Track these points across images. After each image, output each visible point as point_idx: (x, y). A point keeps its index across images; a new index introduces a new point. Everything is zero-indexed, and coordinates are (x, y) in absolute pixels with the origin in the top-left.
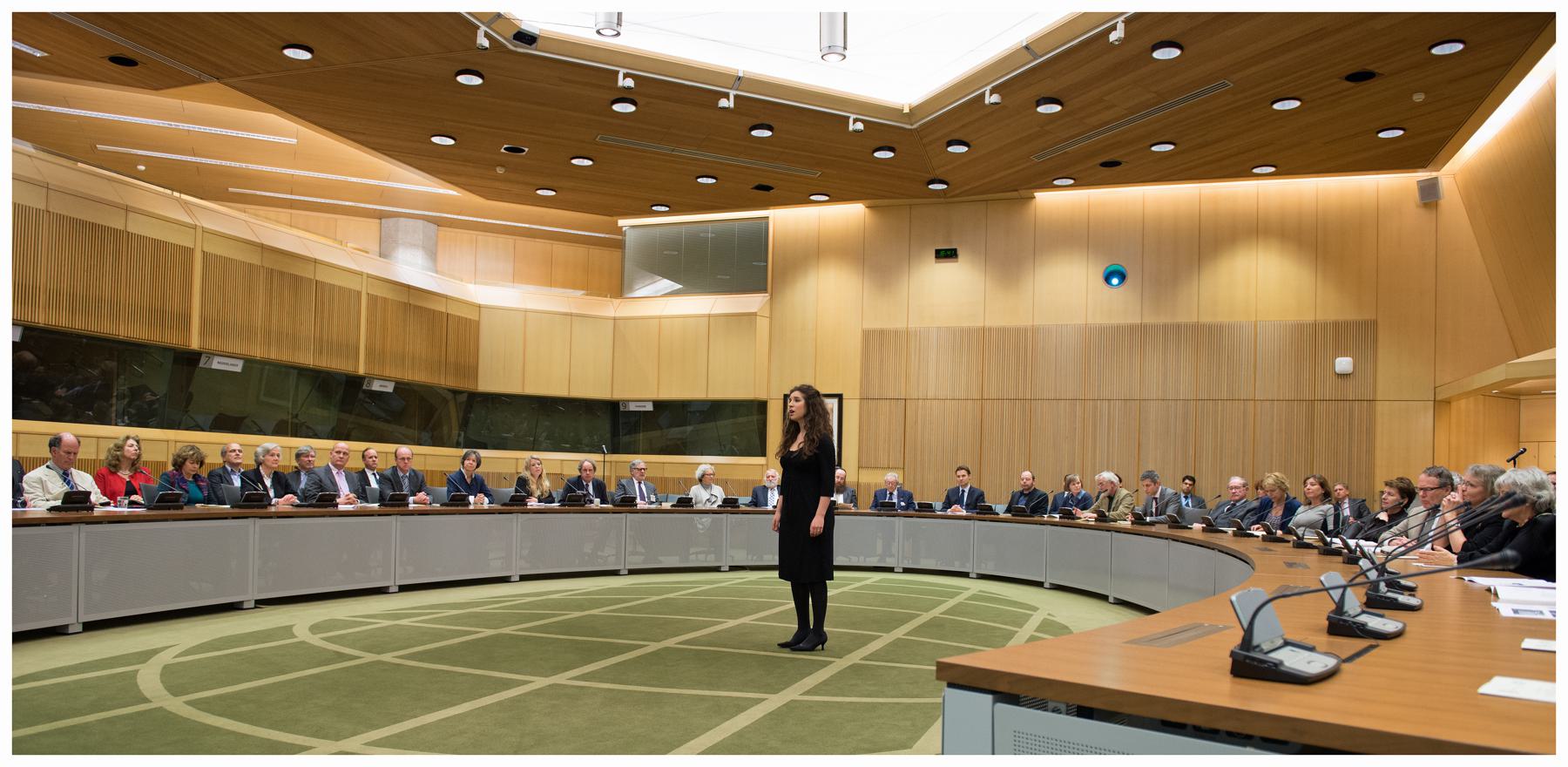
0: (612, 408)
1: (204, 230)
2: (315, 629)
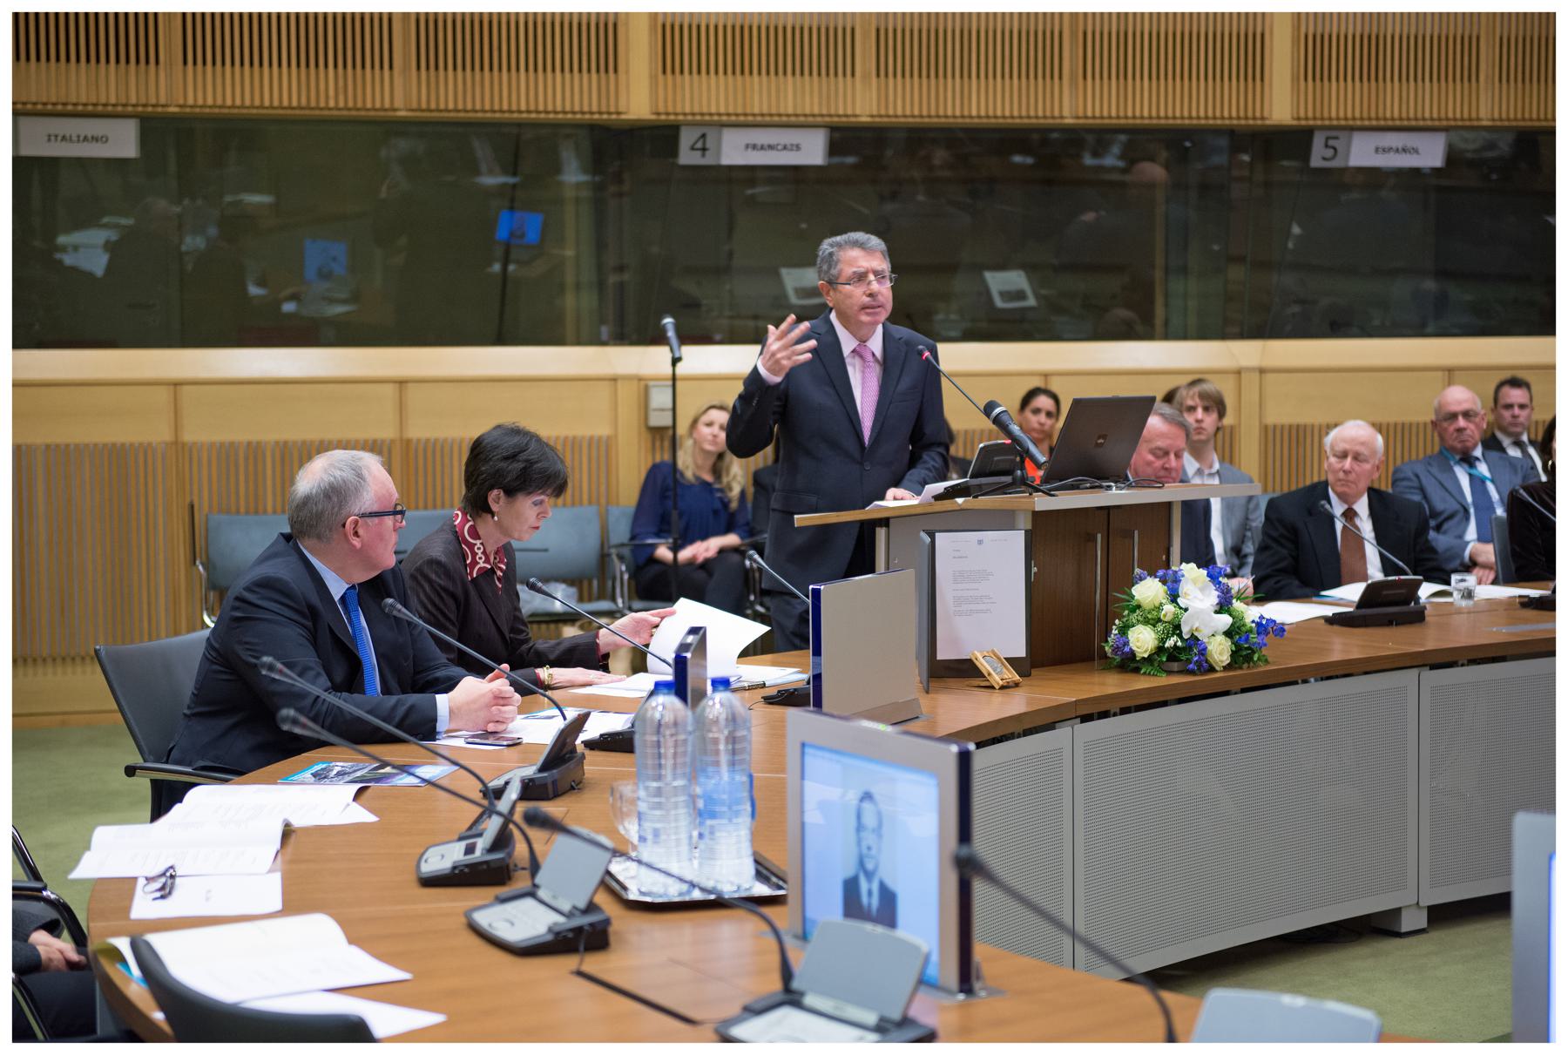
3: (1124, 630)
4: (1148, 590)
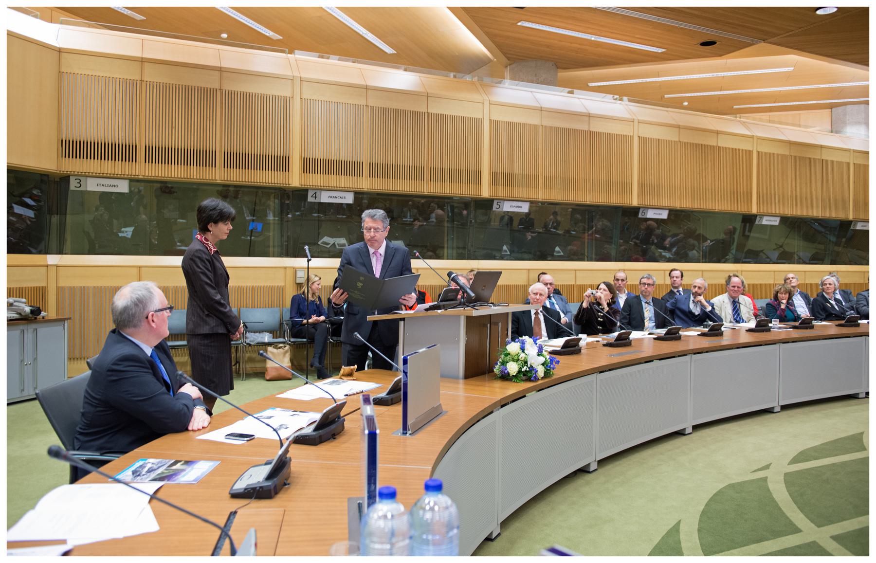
1: (758, 138)
3: (504, 363)
4: (513, 348)
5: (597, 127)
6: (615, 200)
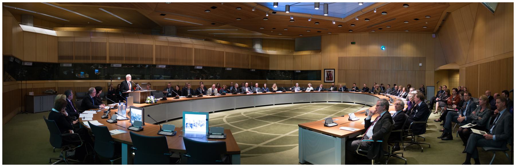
0: (293, 72)
2: (244, 113)
4: (149, 98)
5: (183, 46)
6: (188, 64)
